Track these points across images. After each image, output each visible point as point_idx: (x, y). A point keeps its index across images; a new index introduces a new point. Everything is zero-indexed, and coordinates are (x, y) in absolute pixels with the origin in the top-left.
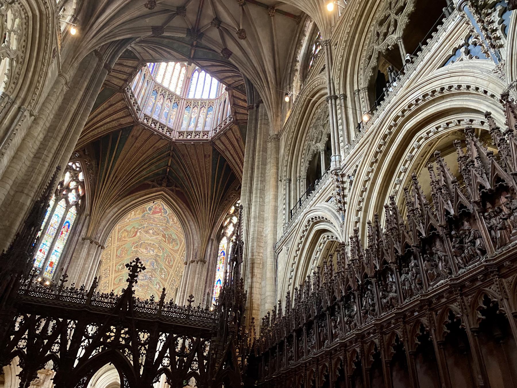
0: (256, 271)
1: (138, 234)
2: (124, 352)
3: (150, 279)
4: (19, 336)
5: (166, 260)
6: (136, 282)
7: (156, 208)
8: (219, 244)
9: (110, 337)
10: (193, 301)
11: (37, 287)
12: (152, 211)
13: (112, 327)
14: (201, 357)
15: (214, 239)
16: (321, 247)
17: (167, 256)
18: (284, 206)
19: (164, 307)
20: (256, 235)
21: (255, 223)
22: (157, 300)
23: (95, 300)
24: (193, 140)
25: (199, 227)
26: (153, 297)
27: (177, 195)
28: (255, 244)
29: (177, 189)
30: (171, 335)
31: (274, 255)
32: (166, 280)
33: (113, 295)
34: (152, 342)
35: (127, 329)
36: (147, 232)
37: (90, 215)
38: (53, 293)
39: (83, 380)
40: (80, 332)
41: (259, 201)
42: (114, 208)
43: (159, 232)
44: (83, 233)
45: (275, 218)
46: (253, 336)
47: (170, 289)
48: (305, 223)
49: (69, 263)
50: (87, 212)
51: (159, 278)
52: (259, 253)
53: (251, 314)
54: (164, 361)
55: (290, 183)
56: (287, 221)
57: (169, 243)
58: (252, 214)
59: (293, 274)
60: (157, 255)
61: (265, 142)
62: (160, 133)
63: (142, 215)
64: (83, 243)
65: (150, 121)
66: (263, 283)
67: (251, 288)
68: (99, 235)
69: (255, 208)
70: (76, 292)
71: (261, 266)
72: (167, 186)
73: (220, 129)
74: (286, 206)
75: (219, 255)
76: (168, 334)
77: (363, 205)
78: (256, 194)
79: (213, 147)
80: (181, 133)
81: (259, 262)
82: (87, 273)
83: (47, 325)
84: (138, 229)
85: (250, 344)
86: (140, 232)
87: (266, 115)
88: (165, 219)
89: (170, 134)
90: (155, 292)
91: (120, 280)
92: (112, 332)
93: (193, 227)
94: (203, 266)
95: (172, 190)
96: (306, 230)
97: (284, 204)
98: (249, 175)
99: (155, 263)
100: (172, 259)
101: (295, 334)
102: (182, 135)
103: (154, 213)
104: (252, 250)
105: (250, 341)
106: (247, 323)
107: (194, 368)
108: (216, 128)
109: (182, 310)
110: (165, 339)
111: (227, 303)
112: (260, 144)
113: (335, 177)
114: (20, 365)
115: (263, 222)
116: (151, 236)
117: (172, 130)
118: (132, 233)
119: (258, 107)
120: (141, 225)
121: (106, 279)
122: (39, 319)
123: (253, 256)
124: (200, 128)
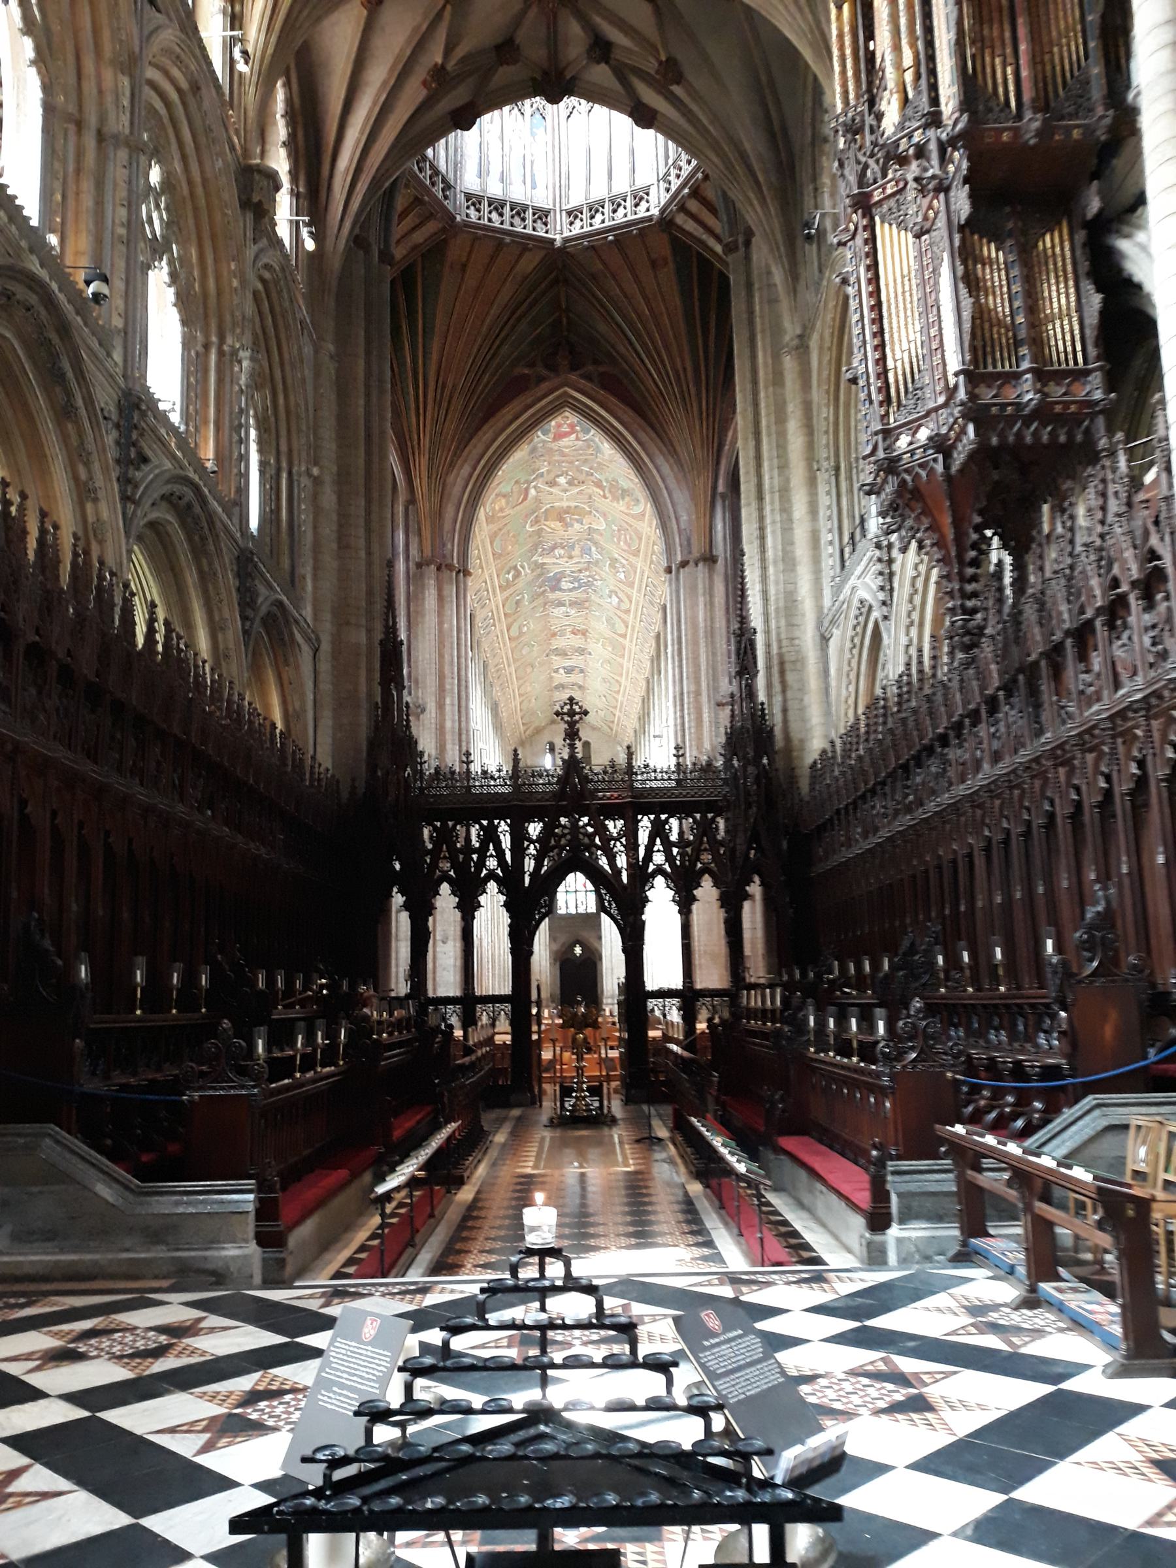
0: (790, 677)
1: (533, 492)
7: (559, 426)
12: (551, 435)
13: (563, 820)
20: (781, 604)
21: (776, 572)
24: (610, 230)
26: (612, 761)
28: (783, 623)
29: (601, 369)
30: (657, 818)
32: (631, 585)
34: (631, 833)
36: (552, 483)
37: (412, 501)
40: (519, 837)
42: (461, 467)
43: (582, 477)
44: (414, 551)
45: (816, 560)
48: (856, 603)
55: (837, 476)
57: (615, 499)
58: (770, 554)
59: (852, 688)
61: (776, 357)
62: (518, 235)
64: (422, 576)
65: (485, 205)
66: (806, 698)
67: (785, 711)
70: (492, 778)
72: (574, 368)
73: (678, 176)
76: (652, 817)
77: (915, 616)
78: (772, 503)
79: (670, 234)
80: (575, 214)
84: (529, 482)
87: (769, 273)
89: (546, 224)
91: (518, 603)
93: (666, 469)
94: (711, 571)
95: (588, 378)
97: (830, 531)
98: (752, 453)
103: (559, 436)
104: (778, 634)
108: (667, 174)
112: (765, 363)
113: (877, 553)
114: (454, 893)
116: (565, 491)
117: (546, 213)
119: (748, 243)
120: (534, 471)
121: (486, 610)
123: (780, 647)
124: (621, 186)
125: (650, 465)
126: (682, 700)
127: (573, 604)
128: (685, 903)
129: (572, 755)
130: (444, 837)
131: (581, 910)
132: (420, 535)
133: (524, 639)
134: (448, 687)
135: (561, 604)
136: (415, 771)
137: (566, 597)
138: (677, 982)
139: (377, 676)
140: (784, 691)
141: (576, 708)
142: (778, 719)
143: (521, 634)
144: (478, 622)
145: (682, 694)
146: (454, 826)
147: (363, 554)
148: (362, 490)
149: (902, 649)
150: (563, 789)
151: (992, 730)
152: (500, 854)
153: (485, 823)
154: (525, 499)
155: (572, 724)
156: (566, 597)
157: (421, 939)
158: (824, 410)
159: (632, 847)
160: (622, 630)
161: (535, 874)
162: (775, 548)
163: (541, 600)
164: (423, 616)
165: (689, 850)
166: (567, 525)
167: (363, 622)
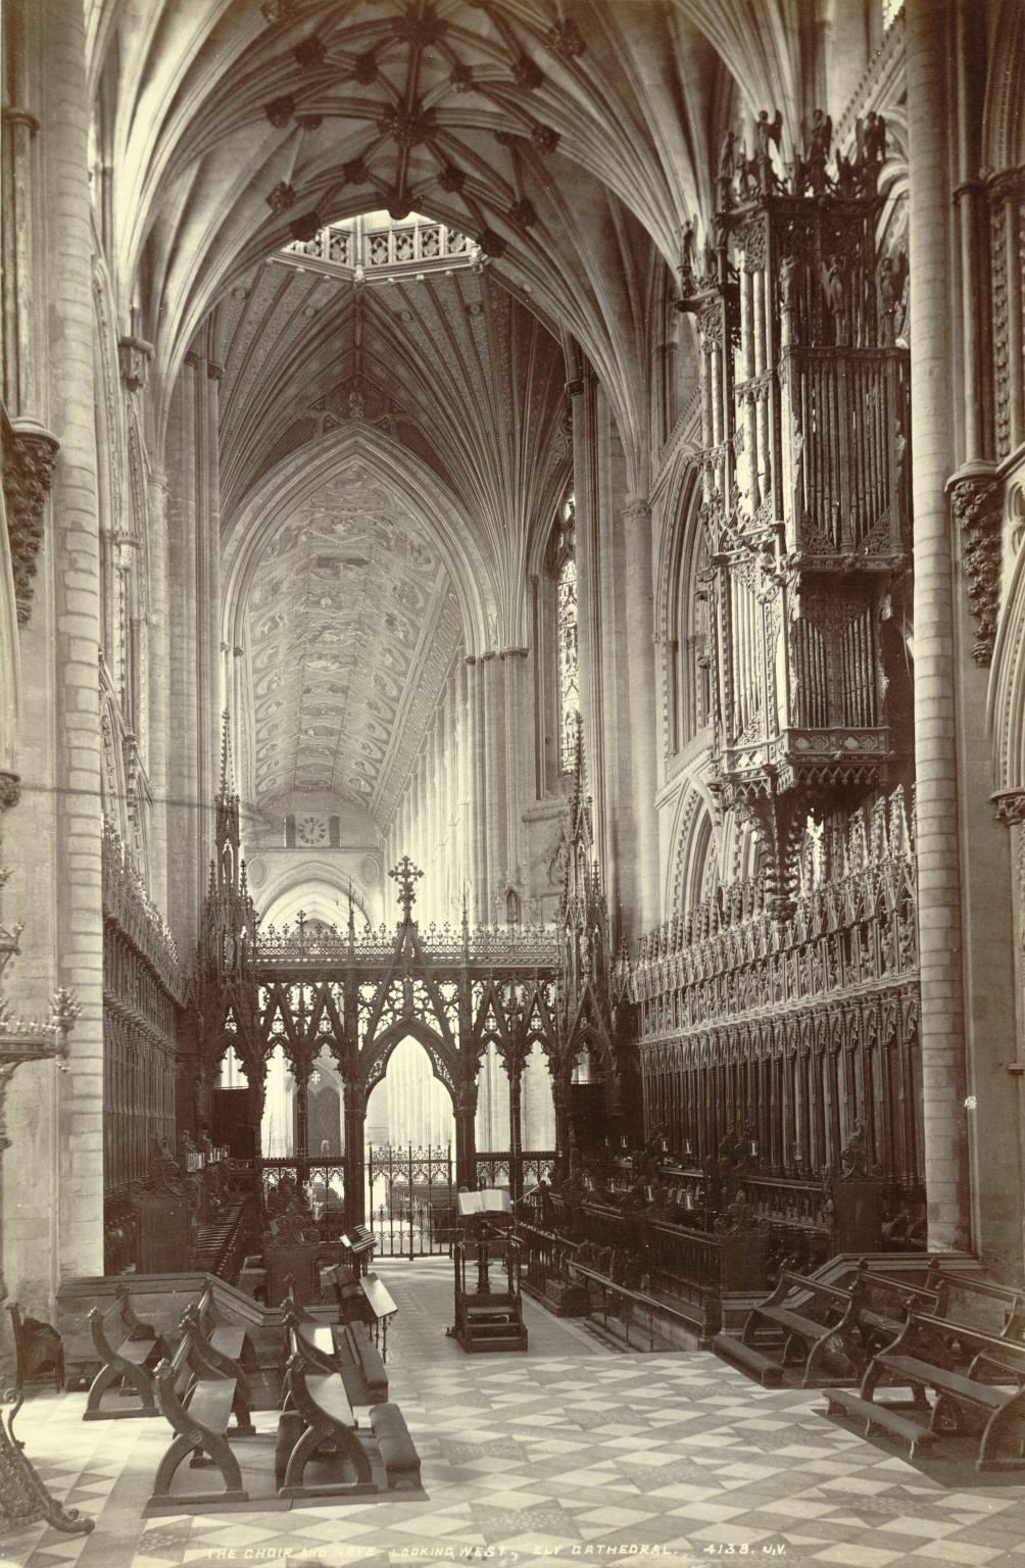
1: (303, 538)
2: (424, 1018)
4: (269, 1013)
13: (397, 984)
15: (540, 577)
27: (401, 440)
48: (689, 792)
78: (610, 667)
83: (301, 994)
94: (521, 667)
102: (380, 245)
111: (574, 924)
114: (287, 1056)
116: (343, 538)
126: (484, 812)
128: (515, 1067)
129: (408, 919)
130: (278, 999)
138: (503, 1145)
145: (484, 805)
147: (194, 700)
148: (194, 631)
149: (731, 856)
158: (664, 586)
160: (394, 693)
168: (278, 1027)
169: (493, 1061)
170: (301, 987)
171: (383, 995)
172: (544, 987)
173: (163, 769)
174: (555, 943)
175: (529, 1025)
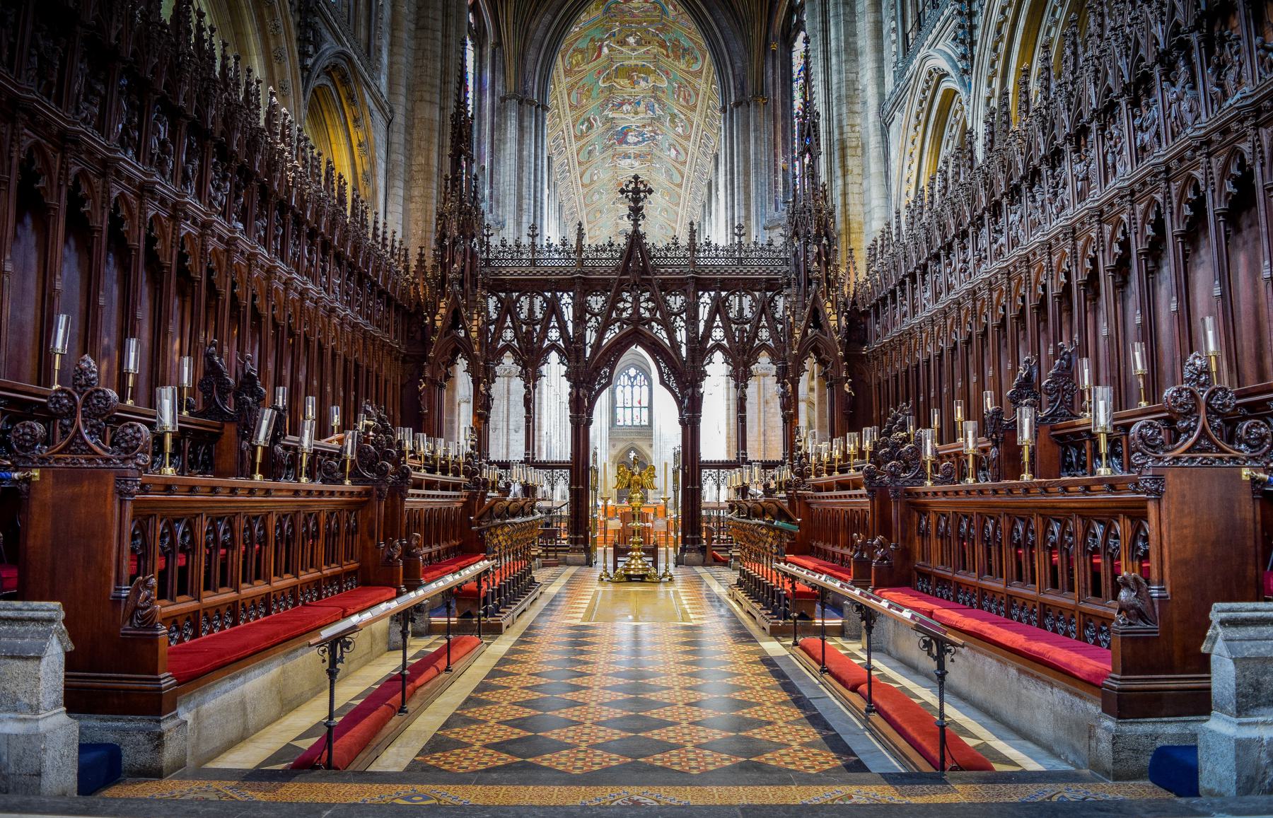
1: (605, 50)
3: (653, 139)
4: (500, 322)
5: (679, 96)
6: (644, 217)
8: (791, 52)
9: (625, 309)
10: (744, 234)
11: (499, 252)
13: (625, 295)
14: (773, 320)
16: (958, 117)
17: (679, 87)
18: (894, 22)
19: (699, 251)
20: (843, 92)
21: (839, 63)
22: (684, 241)
23: (588, 258)
25: (739, 23)
26: (674, 237)
28: (844, 110)
31: (882, 128)
32: (688, 138)
33: (612, 245)
34: (691, 311)
35: (647, 295)
36: (623, 43)
38: (524, 256)
39: (605, 373)
41: (844, 14)
43: (648, 38)
44: (499, 88)
45: (879, 49)
46: (853, 279)
47: (700, 156)
48: (924, 75)
49: (492, 156)
50: (491, 39)
51: (671, 135)
52: (852, 126)
53: (849, 241)
54: (714, 334)
56: (901, 56)
57: (677, 58)
59: (915, 167)
60: (655, 88)
63: (602, 8)
64: (505, 108)
66: (865, 183)
68: (530, 84)
69: (837, 31)
71: (859, 151)
74: (897, 23)
75: (795, 77)
76: (713, 293)
81: (854, 144)
82: (530, 168)
83: (532, 304)
84: (602, 40)
85: (849, 293)
86: (607, 45)
88: (655, 8)
90: (669, 166)
91: (590, 152)
92: (626, 301)
96: (929, 88)
97: (894, 19)
99: (656, 106)
100: (692, 93)
101: (907, 279)
104: (840, 121)
105: (848, 290)
106: (841, 258)
107: (764, 338)
109: (728, 251)
110: (709, 301)
111: (802, 232)
115: (856, 60)
116: (634, 50)
118: (590, 51)
120: (607, 30)
121: (563, 156)
122: (518, 298)
123: (841, 134)
125: (710, 19)
127: (637, 156)
128: (741, 375)
129: (636, 231)
130: (508, 308)
131: (636, 422)
132: (504, 73)
133: (596, 186)
134: (525, 207)
135: (627, 156)
136: (481, 242)
137: (631, 150)
139: (448, 151)
140: (844, 176)
141: (642, 187)
142: (838, 201)
143: (592, 182)
144: (555, 165)
146: (518, 298)
150: (626, 264)
151: (1137, 122)
152: (562, 327)
153: (548, 295)
154: (599, 56)
155: (636, 200)
156: (631, 150)
157: (483, 406)
159: (692, 320)
160: (678, 180)
161: (597, 346)
162: (838, 39)
163: (610, 152)
164: (505, 144)
165: (747, 327)
166: (634, 83)
167: (437, 98)
168: (509, 335)
169: (717, 371)
170: (532, 298)
171: (612, 304)
172: (772, 299)
173: (403, 90)
174: (782, 255)
175: (756, 335)
